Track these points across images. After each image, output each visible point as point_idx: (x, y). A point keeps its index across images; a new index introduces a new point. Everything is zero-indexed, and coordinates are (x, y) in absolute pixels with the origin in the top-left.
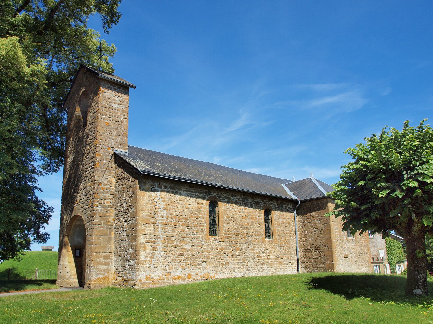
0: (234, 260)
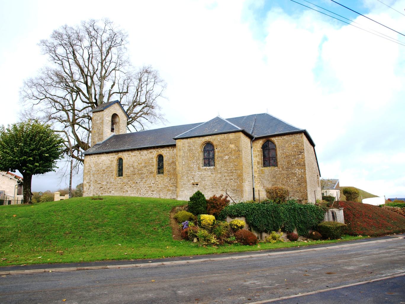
0: (131, 189)
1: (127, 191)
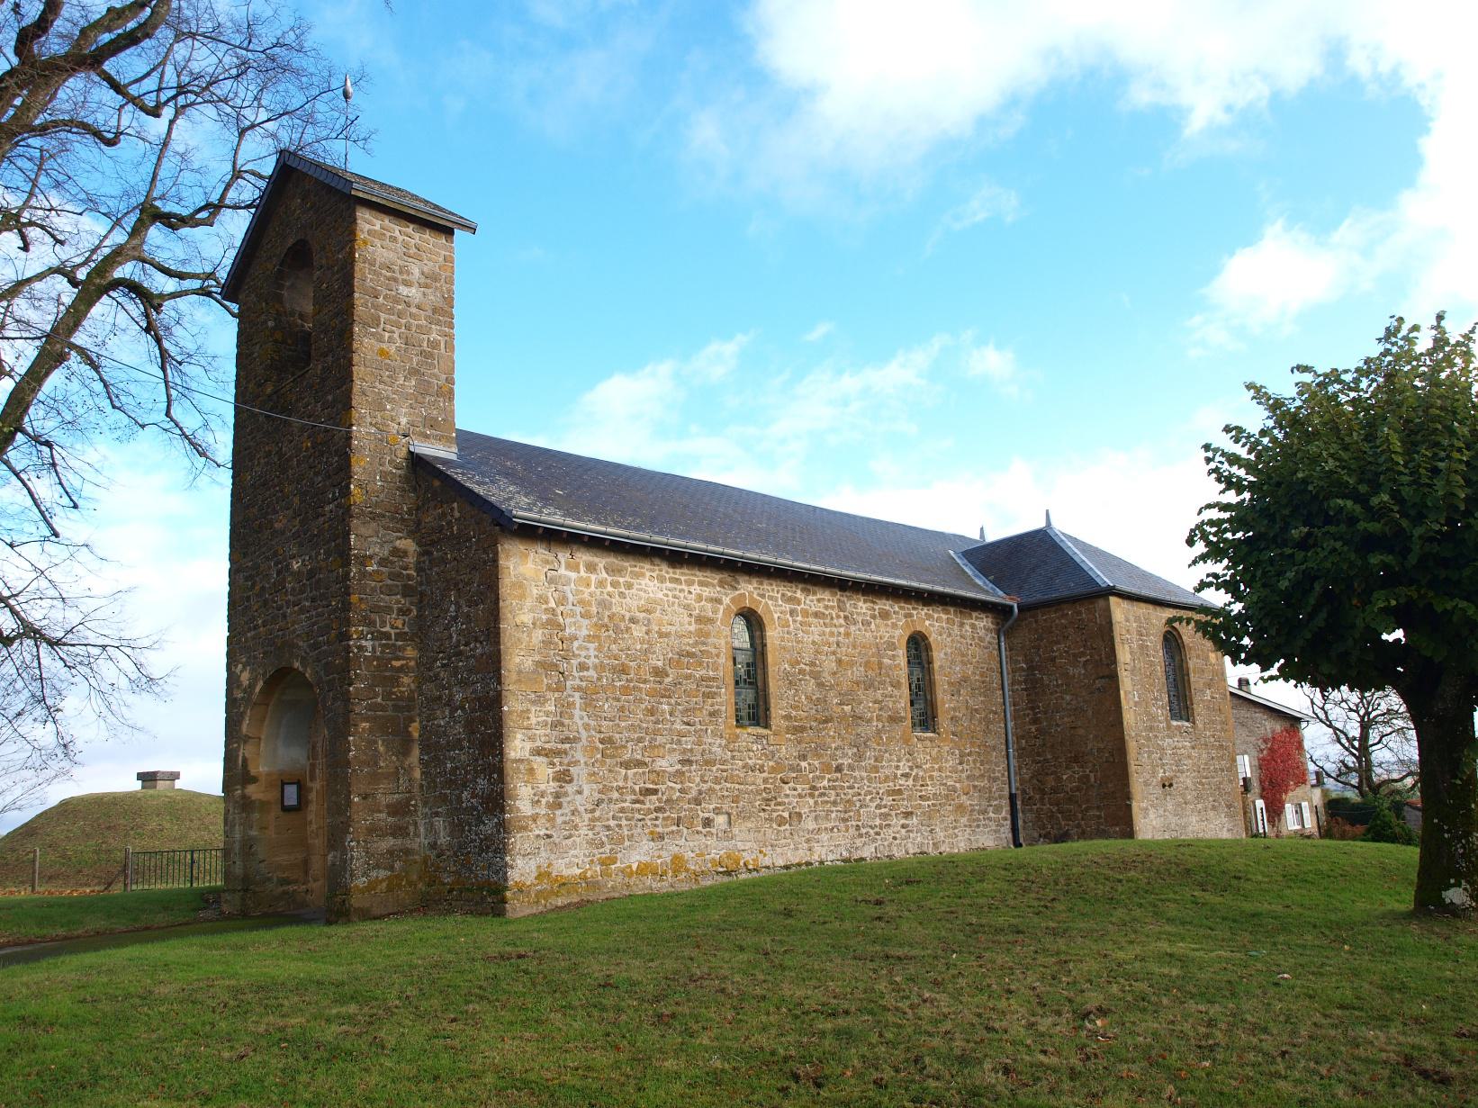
0: (816, 803)
1: (799, 815)
